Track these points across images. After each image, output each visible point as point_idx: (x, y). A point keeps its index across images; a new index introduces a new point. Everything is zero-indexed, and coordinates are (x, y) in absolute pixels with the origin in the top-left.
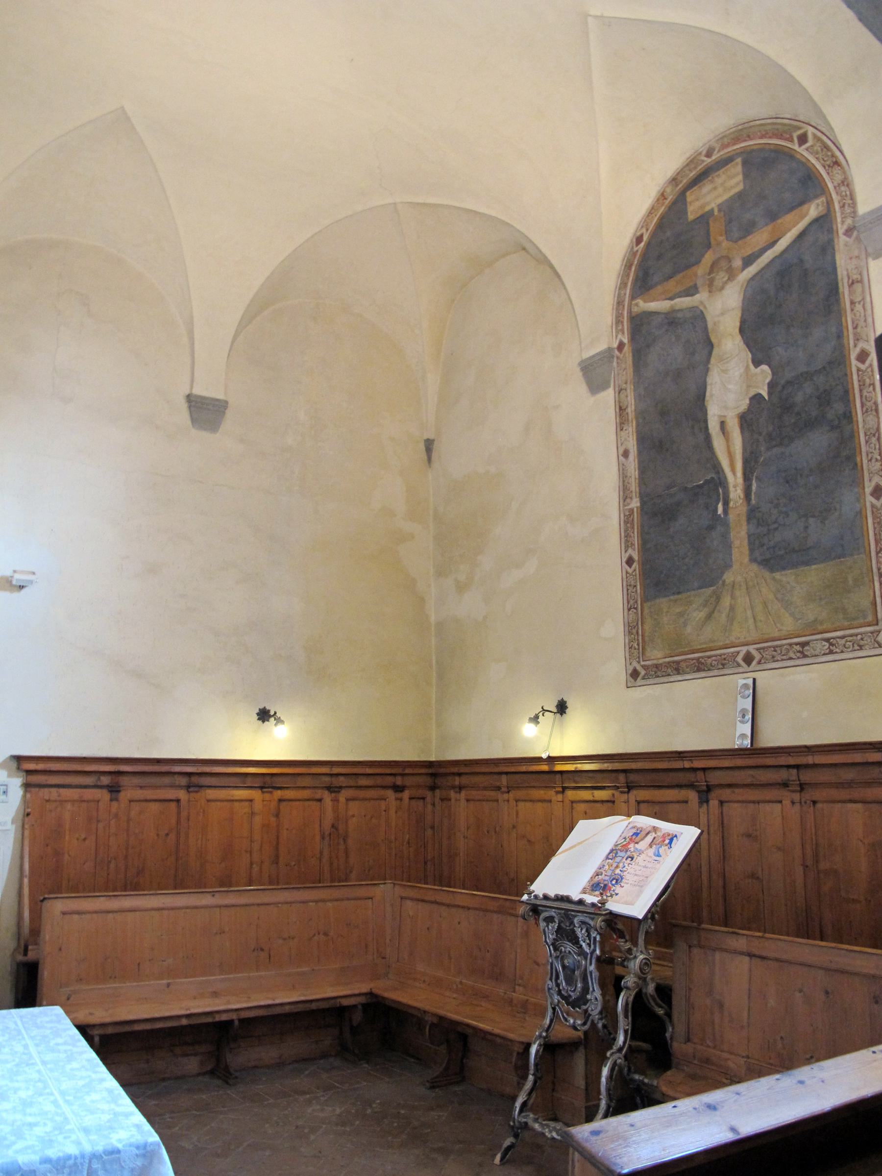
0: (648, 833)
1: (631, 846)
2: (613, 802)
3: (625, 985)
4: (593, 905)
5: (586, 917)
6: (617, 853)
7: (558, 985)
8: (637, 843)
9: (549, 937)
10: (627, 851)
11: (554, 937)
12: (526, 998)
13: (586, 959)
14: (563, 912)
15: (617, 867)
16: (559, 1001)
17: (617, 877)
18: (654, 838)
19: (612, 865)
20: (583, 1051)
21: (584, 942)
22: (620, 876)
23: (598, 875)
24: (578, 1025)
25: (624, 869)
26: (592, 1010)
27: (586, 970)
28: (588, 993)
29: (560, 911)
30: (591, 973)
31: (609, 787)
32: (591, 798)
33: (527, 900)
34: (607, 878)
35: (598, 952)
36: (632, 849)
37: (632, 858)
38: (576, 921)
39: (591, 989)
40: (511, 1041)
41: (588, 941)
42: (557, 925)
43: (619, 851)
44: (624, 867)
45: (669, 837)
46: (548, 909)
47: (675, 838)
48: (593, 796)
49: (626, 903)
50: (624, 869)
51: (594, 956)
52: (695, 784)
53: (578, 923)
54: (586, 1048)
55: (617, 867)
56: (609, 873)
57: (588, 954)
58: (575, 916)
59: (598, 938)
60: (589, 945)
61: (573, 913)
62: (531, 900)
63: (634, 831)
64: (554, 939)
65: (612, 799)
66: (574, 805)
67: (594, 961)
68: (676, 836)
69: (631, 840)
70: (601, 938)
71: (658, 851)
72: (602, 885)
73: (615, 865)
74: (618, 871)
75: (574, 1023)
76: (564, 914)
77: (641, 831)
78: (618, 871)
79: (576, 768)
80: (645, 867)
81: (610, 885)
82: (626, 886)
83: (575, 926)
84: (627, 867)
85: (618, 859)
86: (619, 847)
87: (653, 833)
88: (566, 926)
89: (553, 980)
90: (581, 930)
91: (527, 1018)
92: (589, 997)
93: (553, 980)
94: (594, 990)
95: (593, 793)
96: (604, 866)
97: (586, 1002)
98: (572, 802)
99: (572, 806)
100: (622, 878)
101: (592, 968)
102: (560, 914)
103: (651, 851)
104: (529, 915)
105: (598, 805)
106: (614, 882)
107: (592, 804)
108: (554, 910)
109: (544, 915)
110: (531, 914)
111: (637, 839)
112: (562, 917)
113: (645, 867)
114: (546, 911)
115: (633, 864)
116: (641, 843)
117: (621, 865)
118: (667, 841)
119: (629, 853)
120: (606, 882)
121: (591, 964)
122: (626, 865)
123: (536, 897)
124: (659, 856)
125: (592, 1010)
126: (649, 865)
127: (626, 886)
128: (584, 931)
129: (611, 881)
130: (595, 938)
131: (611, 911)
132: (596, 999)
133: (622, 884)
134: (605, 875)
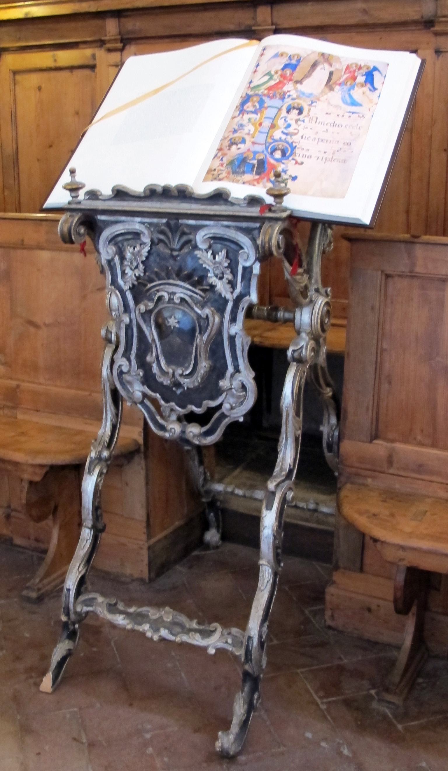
0: (314, 65)
1: (289, 87)
2: (93, 67)
3: (296, 355)
4: (253, 201)
5: (228, 227)
6: (261, 102)
7: (143, 364)
8: (300, 82)
9: (123, 273)
10: (283, 98)
11: (139, 272)
12: (14, 383)
13: (221, 311)
14: (164, 221)
15: (273, 126)
16: (145, 395)
17: (281, 145)
18: (331, 74)
19: (260, 124)
20: (143, 463)
21: (221, 278)
22: (287, 142)
23: (233, 143)
24: (194, 436)
25: (291, 130)
26: (232, 408)
27: (220, 332)
28: (221, 375)
29: (155, 220)
30: (232, 339)
31: (85, 42)
32: (50, 63)
33: (69, 203)
34: (259, 148)
35: (254, 297)
36: (294, 94)
37: (300, 111)
38: (200, 237)
39: (231, 369)
40: (16, 464)
41: (230, 277)
42: (147, 248)
43: (265, 99)
44: (289, 126)
45: (364, 71)
46: (123, 218)
47: (376, 74)
48: (55, 61)
49: (325, 194)
50: (291, 130)
51: (244, 304)
52: (253, 28)
53: (205, 241)
54: (146, 457)
55: (273, 126)
56: (261, 138)
57: (226, 301)
58: (197, 228)
59: (257, 269)
60: (232, 284)
61: (192, 222)
62: (79, 203)
63: (284, 61)
64: (138, 278)
65: (91, 63)
66: (18, 77)
67: (241, 315)
68: (375, 69)
69: (283, 76)
70: (262, 268)
71: (350, 96)
72: (255, 162)
73: (267, 124)
74: (277, 134)
75: (183, 432)
76: (168, 224)
77: (299, 61)
78: (277, 134)
79: (27, 14)
80: (334, 124)
81: (272, 161)
82: (305, 160)
83: (196, 247)
84: (294, 125)
85: (271, 112)
86: (262, 90)
87: (326, 66)
88: (172, 250)
89: (133, 357)
90: (214, 255)
91: (20, 416)
92: (224, 383)
93: (133, 357)
94: (237, 370)
95: (54, 56)
96: (241, 126)
97: (216, 392)
98: (15, 73)
99: (14, 80)
100: (294, 148)
101: (237, 328)
102: (151, 224)
103: (337, 95)
104: (79, 234)
105: (65, 74)
106: (278, 155)
107: (53, 74)
108: (139, 219)
109: (107, 234)
110: (82, 230)
111: (297, 75)
112: (162, 232)
113: (334, 124)
114: (116, 222)
115: (307, 120)
116: (306, 82)
117: (281, 123)
118: (361, 79)
119: (288, 102)
120: (261, 157)
121: (233, 320)
122: (293, 123)
123: (93, 195)
124: (354, 103)
125: (232, 408)
126: (339, 121)
127: (305, 160)
128: (221, 257)
129: (271, 153)
130: (247, 271)
131: (292, 211)
132: (244, 387)
133: (299, 160)
134: (254, 143)
